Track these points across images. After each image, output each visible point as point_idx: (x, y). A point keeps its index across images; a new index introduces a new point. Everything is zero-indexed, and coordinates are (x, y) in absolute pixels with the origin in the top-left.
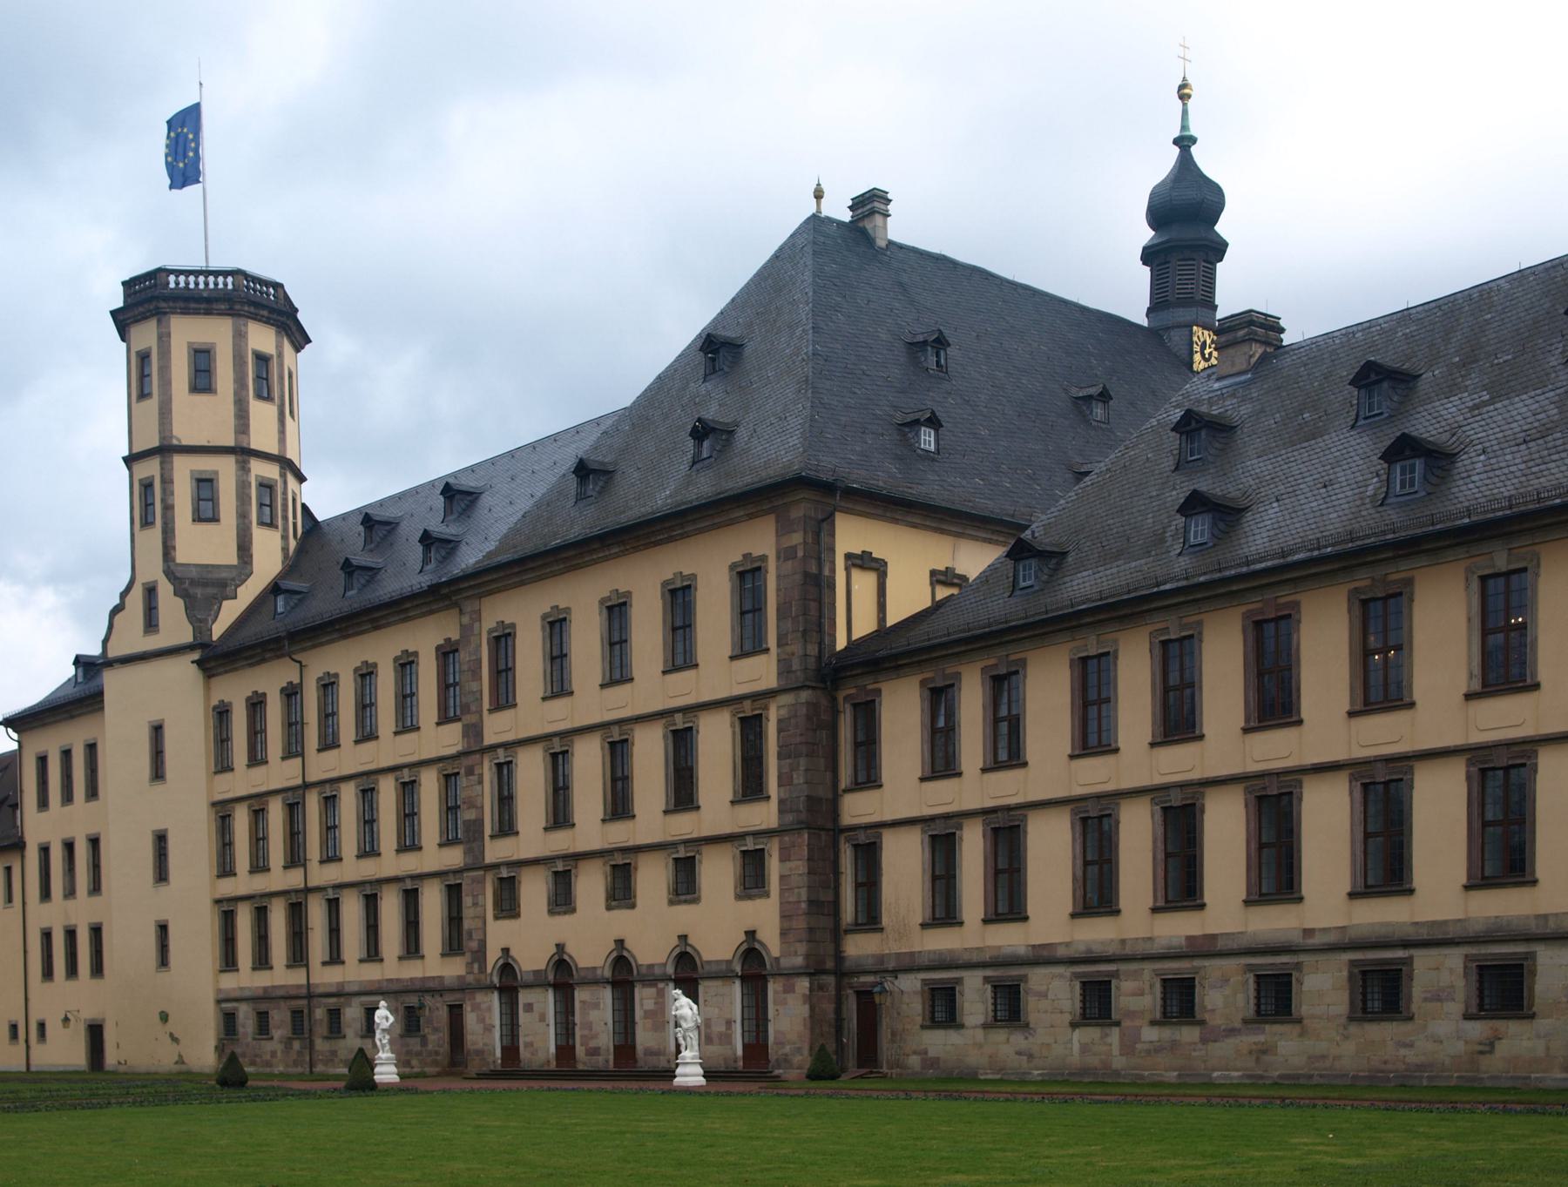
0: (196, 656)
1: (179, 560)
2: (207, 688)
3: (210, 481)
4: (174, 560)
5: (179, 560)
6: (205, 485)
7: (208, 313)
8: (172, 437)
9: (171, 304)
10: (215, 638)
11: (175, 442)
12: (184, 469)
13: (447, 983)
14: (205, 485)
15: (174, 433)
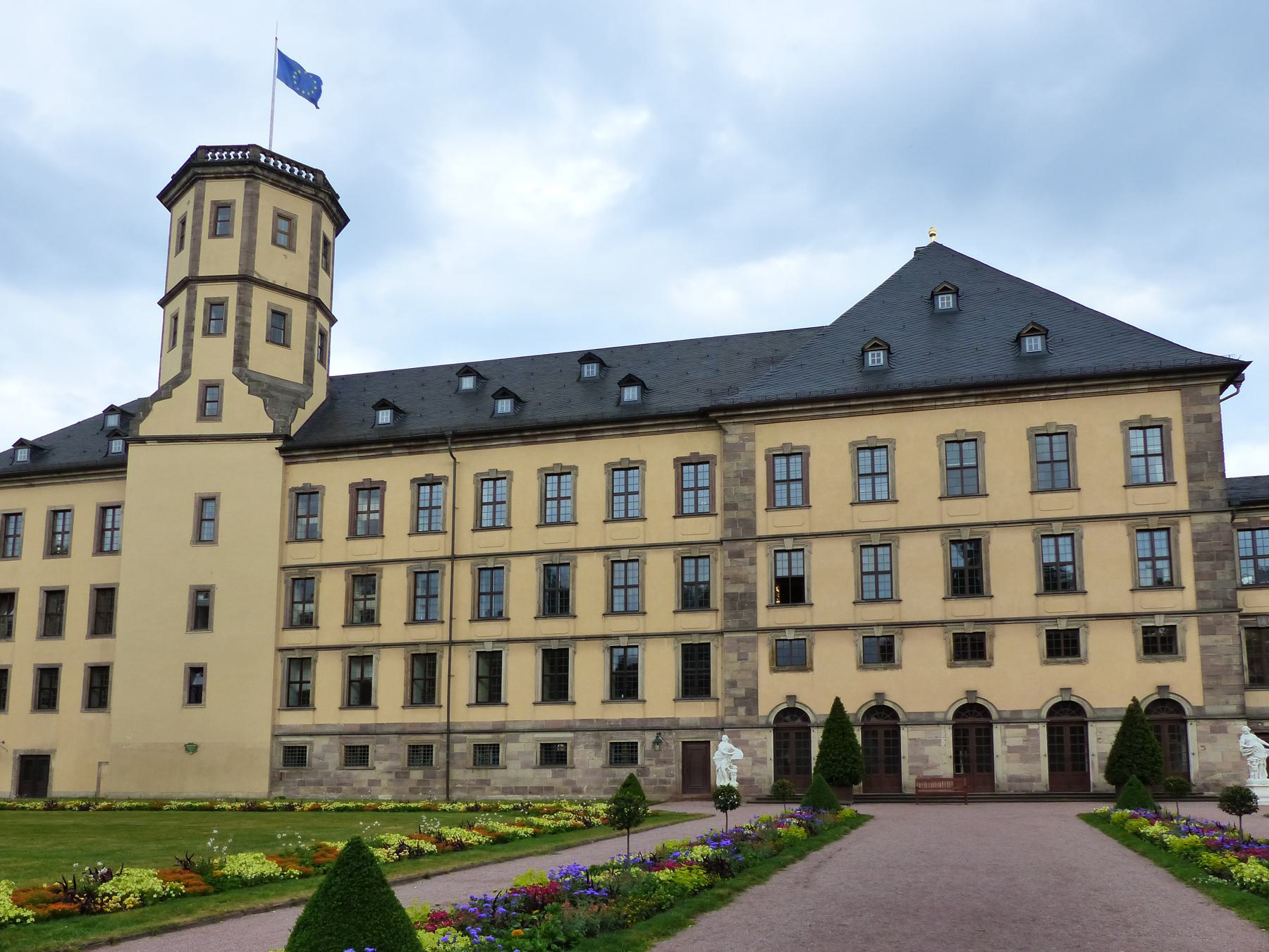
0: (279, 444)
1: (250, 367)
2: (285, 473)
3: (283, 315)
4: (246, 366)
5: (250, 367)
6: (279, 319)
7: (294, 191)
8: (253, 271)
9: (265, 173)
10: (292, 435)
11: (255, 276)
12: (261, 301)
13: (681, 723)
14: (279, 319)
15: (256, 269)
